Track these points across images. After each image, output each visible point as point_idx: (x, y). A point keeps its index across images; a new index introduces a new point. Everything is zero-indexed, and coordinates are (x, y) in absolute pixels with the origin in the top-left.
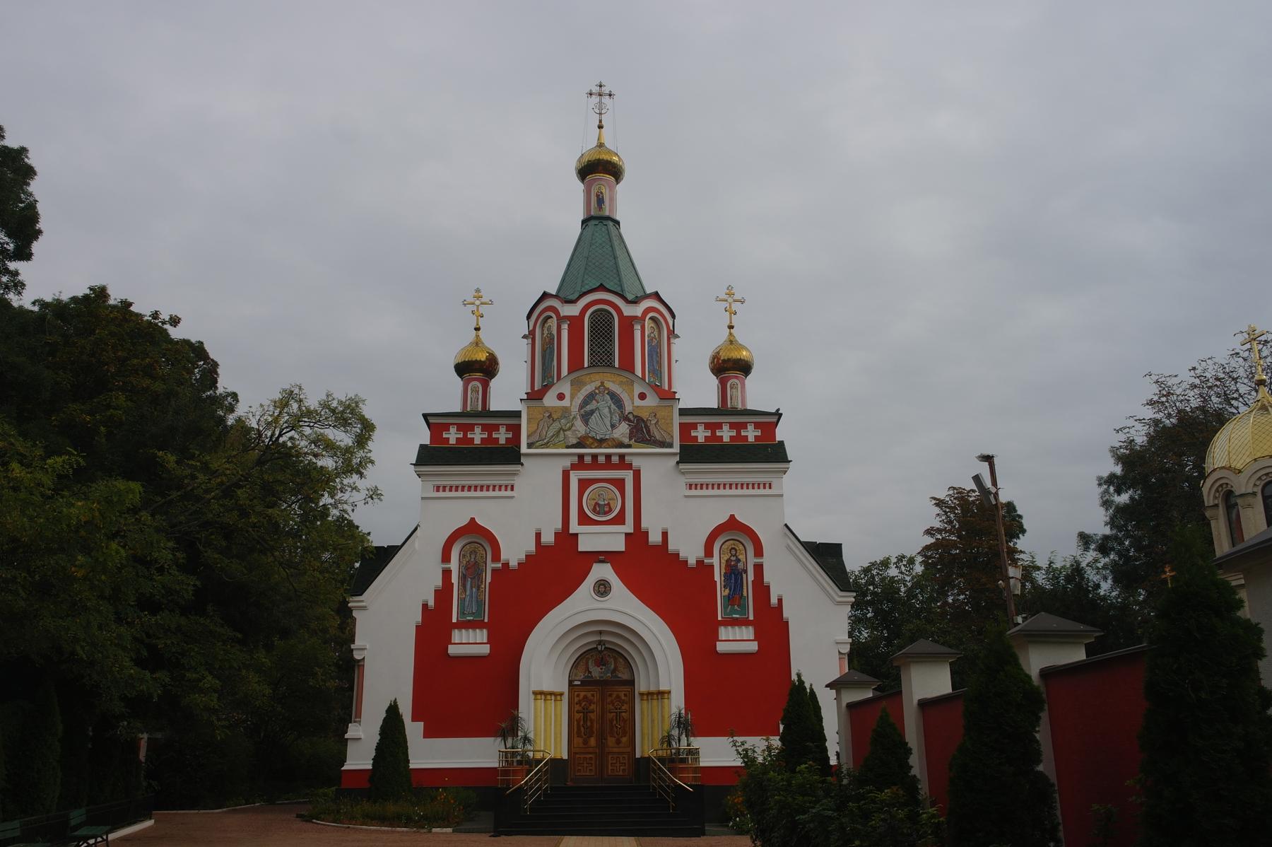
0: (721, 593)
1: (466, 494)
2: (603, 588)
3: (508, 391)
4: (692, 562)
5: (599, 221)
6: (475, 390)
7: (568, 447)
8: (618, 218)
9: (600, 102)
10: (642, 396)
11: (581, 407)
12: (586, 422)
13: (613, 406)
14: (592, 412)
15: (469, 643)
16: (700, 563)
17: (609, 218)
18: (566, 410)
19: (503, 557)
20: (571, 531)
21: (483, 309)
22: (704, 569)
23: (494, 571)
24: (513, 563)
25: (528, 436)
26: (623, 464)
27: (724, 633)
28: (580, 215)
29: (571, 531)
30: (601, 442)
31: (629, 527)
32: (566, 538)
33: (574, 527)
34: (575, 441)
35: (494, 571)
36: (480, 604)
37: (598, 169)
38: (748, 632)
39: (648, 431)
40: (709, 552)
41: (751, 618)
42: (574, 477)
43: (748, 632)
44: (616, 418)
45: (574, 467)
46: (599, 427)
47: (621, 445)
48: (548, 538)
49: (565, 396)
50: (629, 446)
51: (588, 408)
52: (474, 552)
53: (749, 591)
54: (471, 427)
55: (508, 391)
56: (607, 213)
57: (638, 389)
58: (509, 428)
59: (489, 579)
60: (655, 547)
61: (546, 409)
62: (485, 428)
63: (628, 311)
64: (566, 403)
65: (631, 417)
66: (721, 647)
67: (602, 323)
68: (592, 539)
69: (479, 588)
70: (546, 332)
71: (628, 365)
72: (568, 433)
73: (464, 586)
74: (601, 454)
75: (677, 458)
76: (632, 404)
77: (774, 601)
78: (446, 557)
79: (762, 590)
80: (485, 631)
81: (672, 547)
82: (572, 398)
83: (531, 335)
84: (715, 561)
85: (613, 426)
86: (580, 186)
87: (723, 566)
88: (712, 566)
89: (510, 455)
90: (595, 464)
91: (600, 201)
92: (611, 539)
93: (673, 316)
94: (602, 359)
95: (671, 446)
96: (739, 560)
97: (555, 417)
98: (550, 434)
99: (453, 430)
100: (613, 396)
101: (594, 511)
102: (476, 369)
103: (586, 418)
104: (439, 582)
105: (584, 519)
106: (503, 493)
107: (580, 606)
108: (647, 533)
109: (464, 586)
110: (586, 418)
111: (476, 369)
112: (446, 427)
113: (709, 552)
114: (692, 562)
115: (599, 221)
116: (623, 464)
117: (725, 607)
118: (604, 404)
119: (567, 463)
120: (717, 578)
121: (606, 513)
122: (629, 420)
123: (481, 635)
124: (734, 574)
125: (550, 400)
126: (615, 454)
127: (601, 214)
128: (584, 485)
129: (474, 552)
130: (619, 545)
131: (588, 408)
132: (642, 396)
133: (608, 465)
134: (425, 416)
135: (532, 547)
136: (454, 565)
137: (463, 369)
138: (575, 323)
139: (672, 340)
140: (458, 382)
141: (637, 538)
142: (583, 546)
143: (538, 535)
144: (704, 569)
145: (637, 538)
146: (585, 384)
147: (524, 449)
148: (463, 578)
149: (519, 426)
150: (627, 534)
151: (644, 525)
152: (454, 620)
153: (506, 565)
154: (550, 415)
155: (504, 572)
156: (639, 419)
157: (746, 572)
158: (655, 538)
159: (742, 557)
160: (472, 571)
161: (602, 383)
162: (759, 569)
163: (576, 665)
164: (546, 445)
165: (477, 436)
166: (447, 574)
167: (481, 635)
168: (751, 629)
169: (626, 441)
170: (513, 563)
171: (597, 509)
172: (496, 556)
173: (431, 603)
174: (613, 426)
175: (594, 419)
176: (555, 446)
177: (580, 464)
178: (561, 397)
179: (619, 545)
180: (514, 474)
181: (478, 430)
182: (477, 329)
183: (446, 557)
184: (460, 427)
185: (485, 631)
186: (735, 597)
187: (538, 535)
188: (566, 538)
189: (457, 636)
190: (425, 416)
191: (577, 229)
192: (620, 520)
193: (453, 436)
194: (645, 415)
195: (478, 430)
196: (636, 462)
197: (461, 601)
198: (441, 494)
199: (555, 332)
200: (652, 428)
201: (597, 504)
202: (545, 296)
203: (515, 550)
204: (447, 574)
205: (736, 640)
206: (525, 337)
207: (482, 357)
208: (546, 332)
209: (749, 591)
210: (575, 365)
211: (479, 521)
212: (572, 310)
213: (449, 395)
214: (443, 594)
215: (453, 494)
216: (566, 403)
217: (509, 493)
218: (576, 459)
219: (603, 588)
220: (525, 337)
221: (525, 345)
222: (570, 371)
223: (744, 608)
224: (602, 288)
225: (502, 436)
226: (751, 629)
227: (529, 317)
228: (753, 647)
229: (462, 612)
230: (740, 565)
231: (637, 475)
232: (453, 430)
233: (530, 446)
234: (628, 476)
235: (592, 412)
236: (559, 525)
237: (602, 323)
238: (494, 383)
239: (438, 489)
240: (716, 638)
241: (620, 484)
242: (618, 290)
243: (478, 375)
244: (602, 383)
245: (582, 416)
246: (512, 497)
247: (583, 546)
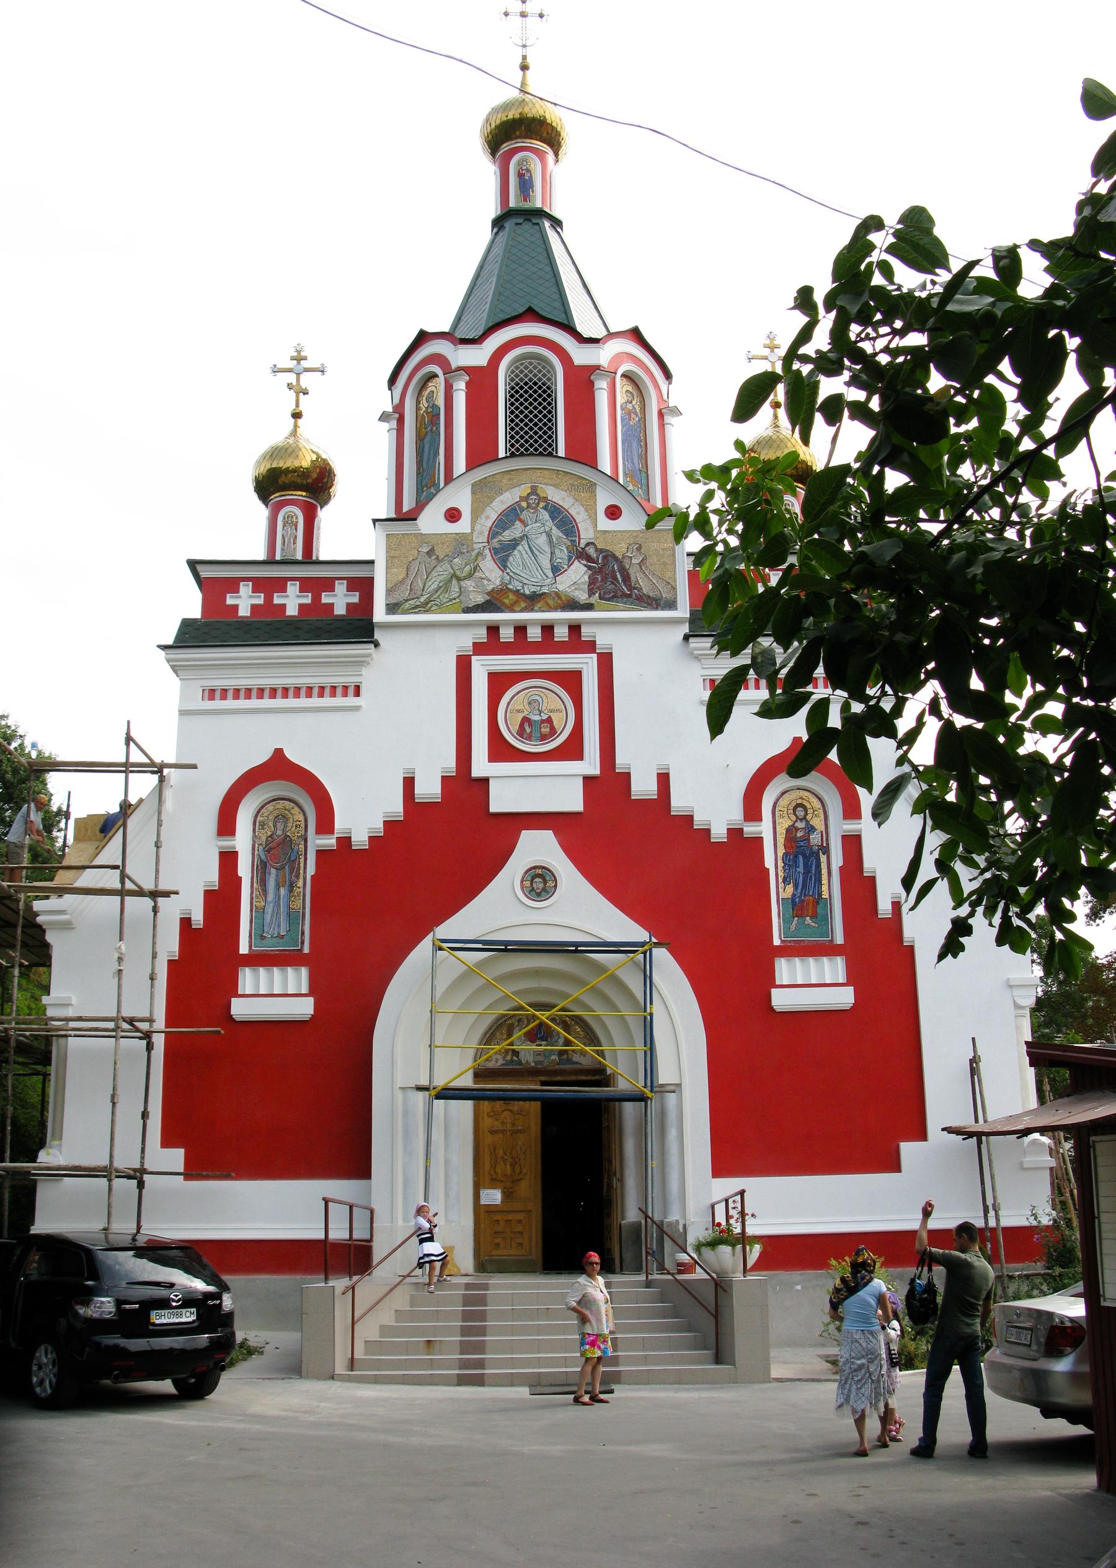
0: (778, 891)
1: (267, 703)
2: (540, 882)
3: (349, 530)
4: (719, 833)
5: (523, 222)
6: (290, 522)
7: (467, 610)
8: (556, 213)
9: (524, 28)
10: (613, 512)
11: (493, 534)
12: (503, 564)
13: (556, 532)
14: (514, 544)
15: (275, 995)
16: (735, 833)
17: (541, 213)
18: (461, 543)
19: (340, 824)
21: (306, 380)
22: (743, 846)
23: (321, 854)
24: (360, 839)
25: (389, 591)
26: (577, 642)
27: (785, 970)
28: (492, 210)
30: (533, 601)
31: (590, 765)
32: (464, 788)
34: (480, 599)
35: (321, 854)
36: (293, 918)
37: (519, 133)
38: (834, 968)
39: (627, 578)
40: (752, 811)
41: (839, 939)
42: (481, 669)
43: (834, 968)
44: (562, 554)
45: (479, 649)
46: (529, 570)
47: (573, 605)
48: (429, 788)
49: (460, 507)
50: (589, 607)
51: (508, 535)
52: (282, 817)
53: (833, 889)
54: (280, 584)
55: (349, 530)
56: (539, 205)
57: (604, 500)
58: (354, 584)
59: (311, 870)
60: (644, 803)
61: (423, 538)
62: (306, 585)
63: (581, 356)
64: (463, 526)
65: (591, 551)
66: (781, 1000)
67: (531, 396)
68: (512, 789)
69: (291, 887)
70: (424, 404)
71: (583, 450)
72: (469, 584)
73: (263, 883)
74: (534, 622)
75: (686, 629)
76: (593, 527)
78: (226, 825)
80: (304, 971)
81: (678, 803)
82: (476, 515)
83: (399, 409)
84: (764, 829)
85: (556, 570)
86: (487, 171)
87: (781, 840)
88: (758, 841)
89: (358, 628)
90: (521, 644)
91: (525, 185)
92: (560, 788)
93: (668, 375)
94: (533, 440)
95: (671, 605)
96: (811, 829)
97: (440, 552)
98: (432, 586)
99: (245, 589)
100: (555, 512)
102: (295, 485)
103: (502, 554)
104: (212, 876)
105: (500, 750)
106: (339, 701)
107: (496, 910)
108: (628, 775)
109: (263, 883)
110: (502, 554)
111: (295, 485)
112: (233, 585)
113: (752, 811)
114: (719, 833)
115: (523, 222)
116: (577, 642)
117: (786, 922)
118: (539, 529)
119: (465, 641)
120: (769, 862)
121: (543, 738)
122: (589, 558)
123: (297, 979)
124: (802, 853)
125: (431, 521)
126: (561, 622)
127: (527, 205)
128: (499, 683)
129: (282, 817)
130: (572, 800)
131: (508, 535)
132: (613, 512)
133: (548, 643)
134: (193, 564)
135: (396, 807)
136: (243, 841)
137: (270, 485)
138: (481, 381)
139: (668, 419)
140: (261, 512)
141: (607, 786)
142: (500, 801)
143: (409, 783)
144: (743, 846)
145: (607, 786)
146: (500, 492)
147: (380, 614)
148: (261, 870)
149: (371, 580)
150: (587, 780)
152: (244, 949)
153: (345, 842)
154: (432, 549)
156: (608, 556)
157: (826, 850)
158: (643, 786)
159: (818, 823)
160: (277, 853)
161: (534, 491)
164: (424, 608)
165: (292, 601)
166: (228, 859)
167: (297, 979)
168: (840, 962)
169: (582, 597)
170: (360, 839)
171: (525, 728)
172: (326, 823)
173: (198, 918)
174: (556, 570)
175: (517, 558)
176: (441, 609)
177: (492, 644)
178: (453, 515)
179: (572, 800)
180: (360, 663)
181: (293, 589)
182: (297, 415)
183: (226, 825)
184: (259, 584)
185: (304, 971)
186: (808, 902)
187: (409, 783)
188: (464, 788)
189: (248, 979)
190: (193, 564)
191: (486, 233)
192: (572, 749)
193: (244, 601)
194: (619, 550)
195: (293, 589)
196: (604, 639)
197: (257, 913)
198: (218, 704)
199: (441, 402)
200: (635, 573)
201: (526, 720)
202: (423, 337)
203: (363, 812)
204: (228, 859)
205: (809, 984)
206: (384, 417)
207: (305, 461)
208: (424, 404)
209: (833, 889)
210: (481, 452)
211: (290, 755)
212: (477, 356)
213: (243, 532)
214: (222, 900)
215: (242, 703)
216: (463, 526)
217: (351, 700)
218: (482, 635)
219: (540, 882)
220: (384, 417)
221: (384, 434)
222: (471, 466)
223: (825, 921)
224: (531, 315)
225: (340, 600)
226: (840, 962)
227: (392, 381)
228: (845, 997)
229: (258, 934)
230: (815, 839)
231: (606, 663)
232: (245, 589)
233: (392, 608)
234: (588, 665)
235: (514, 544)
236: (449, 762)
237: (531, 396)
238: (325, 516)
239: (211, 694)
240: (769, 980)
241: (571, 681)
242: (561, 318)
243: (300, 495)
244: (534, 491)
245: (495, 552)
246: (357, 708)
247: (500, 801)
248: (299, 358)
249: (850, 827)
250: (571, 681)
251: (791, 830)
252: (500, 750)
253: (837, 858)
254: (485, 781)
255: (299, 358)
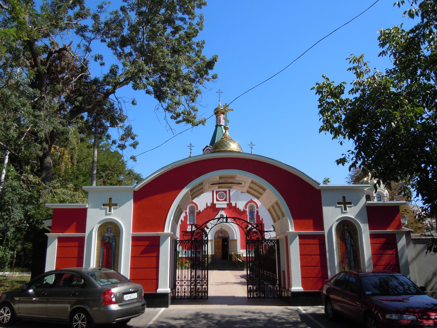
4: (242, 210)
19: (199, 209)
20: (215, 203)
22: (245, 212)
24: (201, 211)
29: (215, 203)
32: (213, 205)
33: (215, 202)
40: (246, 208)
48: (209, 205)
77: (261, 219)
79: (258, 217)
81: (237, 207)
84: (247, 210)
101: (219, 198)
113: (246, 208)
114: (242, 210)
124: (252, 212)
130: (225, 206)
135: (205, 207)
141: (229, 205)
142: (217, 206)
143: (207, 204)
145: (229, 205)
148: (190, 214)
150: (227, 204)
151: (231, 202)
153: (200, 211)
155: (199, 213)
162: (257, 212)
163: (216, 233)
170: (201, 211)
172: (197, 209)
173: (183, 220)
179: (225, 206)
187: (207, 204)
188: (213, 205)
192: (225, 200)
202: (207, 146)
227: (203, 150)
230: (253, 211)
236: (212, 202)
241: (225, 192)
247: (217, 206)
248: (191, 145)
249: (257, 210)
250: (225, 192)
251: (250, 210)
252: (217, 200)
253: (256, 213)
254: (215, 204)
255: (191, 145)
